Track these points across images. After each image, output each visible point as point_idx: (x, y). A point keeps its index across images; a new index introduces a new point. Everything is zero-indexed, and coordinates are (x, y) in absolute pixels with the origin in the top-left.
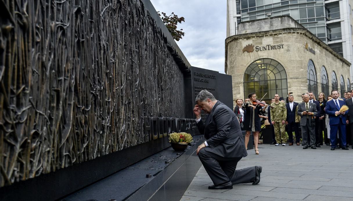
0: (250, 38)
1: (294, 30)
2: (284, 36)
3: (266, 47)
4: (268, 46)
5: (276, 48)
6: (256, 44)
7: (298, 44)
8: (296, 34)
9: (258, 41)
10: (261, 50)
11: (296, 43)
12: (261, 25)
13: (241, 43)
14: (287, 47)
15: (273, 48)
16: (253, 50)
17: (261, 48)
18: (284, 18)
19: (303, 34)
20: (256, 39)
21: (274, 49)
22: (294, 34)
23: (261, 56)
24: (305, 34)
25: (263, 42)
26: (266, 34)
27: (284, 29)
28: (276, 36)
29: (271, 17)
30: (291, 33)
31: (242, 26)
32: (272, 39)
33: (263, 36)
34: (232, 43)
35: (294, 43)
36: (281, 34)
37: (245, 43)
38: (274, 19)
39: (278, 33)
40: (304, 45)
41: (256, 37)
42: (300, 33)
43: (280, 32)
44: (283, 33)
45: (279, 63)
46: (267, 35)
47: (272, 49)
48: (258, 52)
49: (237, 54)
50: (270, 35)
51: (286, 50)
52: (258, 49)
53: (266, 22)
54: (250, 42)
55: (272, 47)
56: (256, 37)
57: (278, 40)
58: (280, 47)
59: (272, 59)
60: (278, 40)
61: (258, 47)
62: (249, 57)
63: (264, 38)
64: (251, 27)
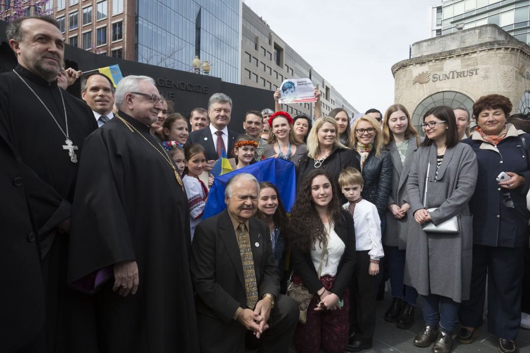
0: (425, 62)
1: (499, 44)
2: (482, 56)
3: (449, 74)
4: (453, 72)
5: (465, 75)
6: (434, 71)
7: (505, 66)
8: (502, 51)
9: (438, 66)
10: (441, 79)
11: (502, 66)
12: (445, 44)
13: (411, 71)
14: (484, 72)
15: (460, 75)
16: (429, 81)
17: (441, 76)
18: (484, 28)
19: (518, 50)
20: (435, 64)
21: (461, 77)
22: (498, 51)
23: (440, 88)
24: (521, 51)
25: (444, 68)
26: (450, 54)
27: (481, 45)
28: (467, 57)
29: (464, 29)
30: (493, 49)
31: (416, 48)
32: (460, 61)
33: (445, 59)
34: (399, 72)
35: (498, 65)
36: (476, 52)
37: (417, 70)
38: (467, 33)
39: (471, 52)
40: (516, 67)
41: (434, 61)
42: (510, 49)
43: (473, 49)
44: (480, 51)
45: (468, 97)
46: (453, 57)
47: (459, 76)
48: (436, 82)
49: (404, 86)
50: (457, 56)
51: (482, 77)
52: (436, 79)
53: (454, 39)
54: (425, 68)
55: (459, 73)
56: (434, 61)
57: (470, 62)
58: (473, 73)
59: (457, 92)
60: (470, 62)
61: (437, 75)
62: (422, 91)
63: (447, 61)
64: (429, 48)
